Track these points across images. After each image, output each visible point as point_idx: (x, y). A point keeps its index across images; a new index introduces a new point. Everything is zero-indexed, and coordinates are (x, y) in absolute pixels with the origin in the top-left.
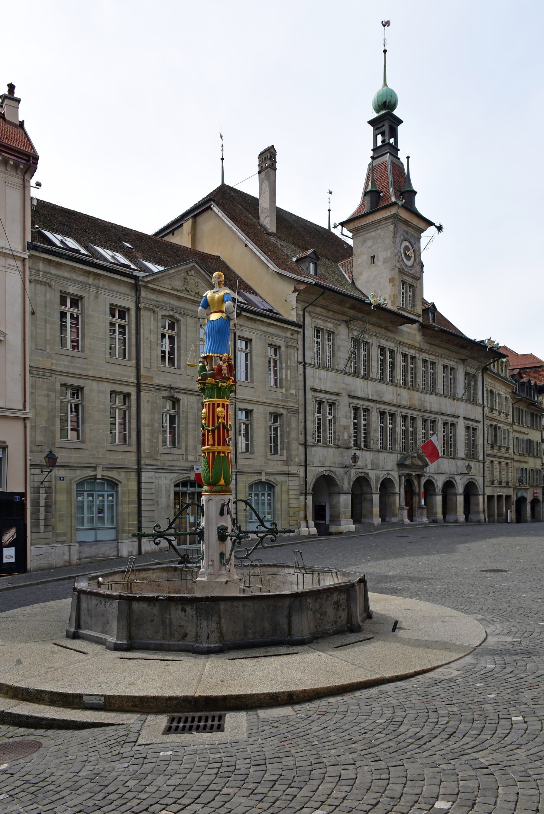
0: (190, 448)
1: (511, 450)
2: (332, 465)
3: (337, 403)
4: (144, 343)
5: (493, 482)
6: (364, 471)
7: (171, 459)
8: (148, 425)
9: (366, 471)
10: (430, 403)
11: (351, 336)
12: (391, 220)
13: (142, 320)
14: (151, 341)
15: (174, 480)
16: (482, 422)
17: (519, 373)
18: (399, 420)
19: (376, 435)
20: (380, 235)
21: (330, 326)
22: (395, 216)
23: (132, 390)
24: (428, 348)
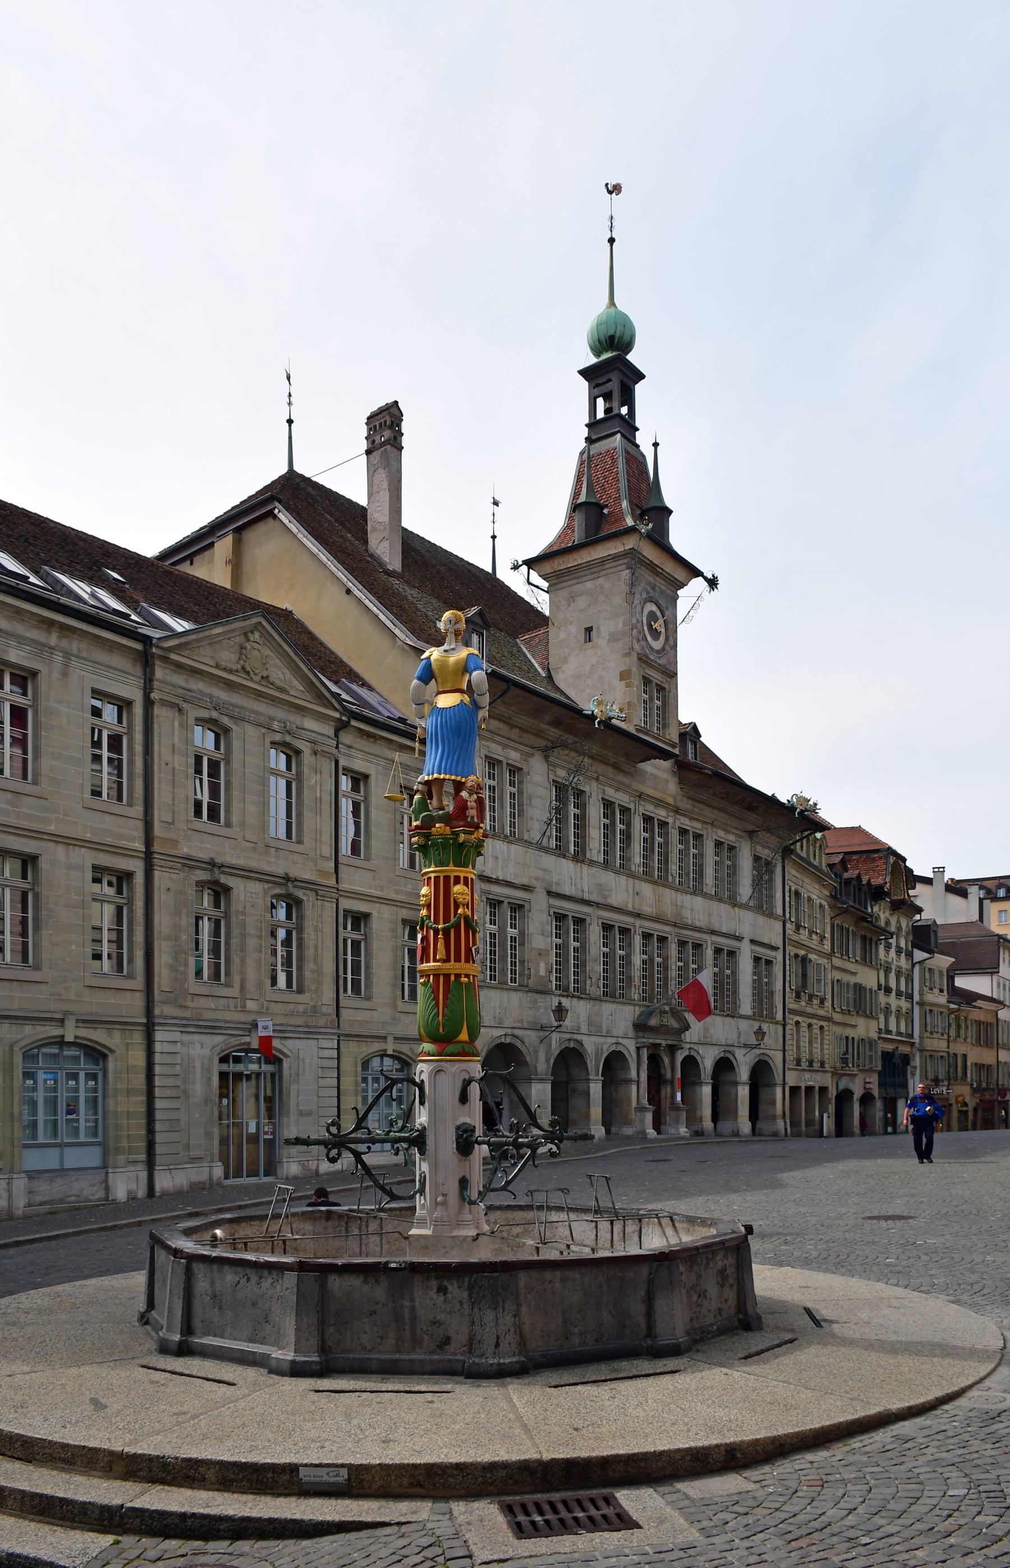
0: (250, 986)
1: (828, 1004)
2: (516, 1025)
3: (527, 906)
4: (160, 772)
5: (798, 1062)
6: (575, 1037)
7: (213, 1007)
8: (168, 938)
9: (579, 1037)
10: (692, 910)
11: (552, 777)
12: (625, 561)
13: (156, 726)
14: (174, 768)
15: (218, 1049)
16: (781, 950)
17: (843, 862)
18: (637, 940)
19: (596, 968)
20: (602, 587)
21: (514, 756)
22: (632, 553)
23: (137, 867)
24: (689, 807)
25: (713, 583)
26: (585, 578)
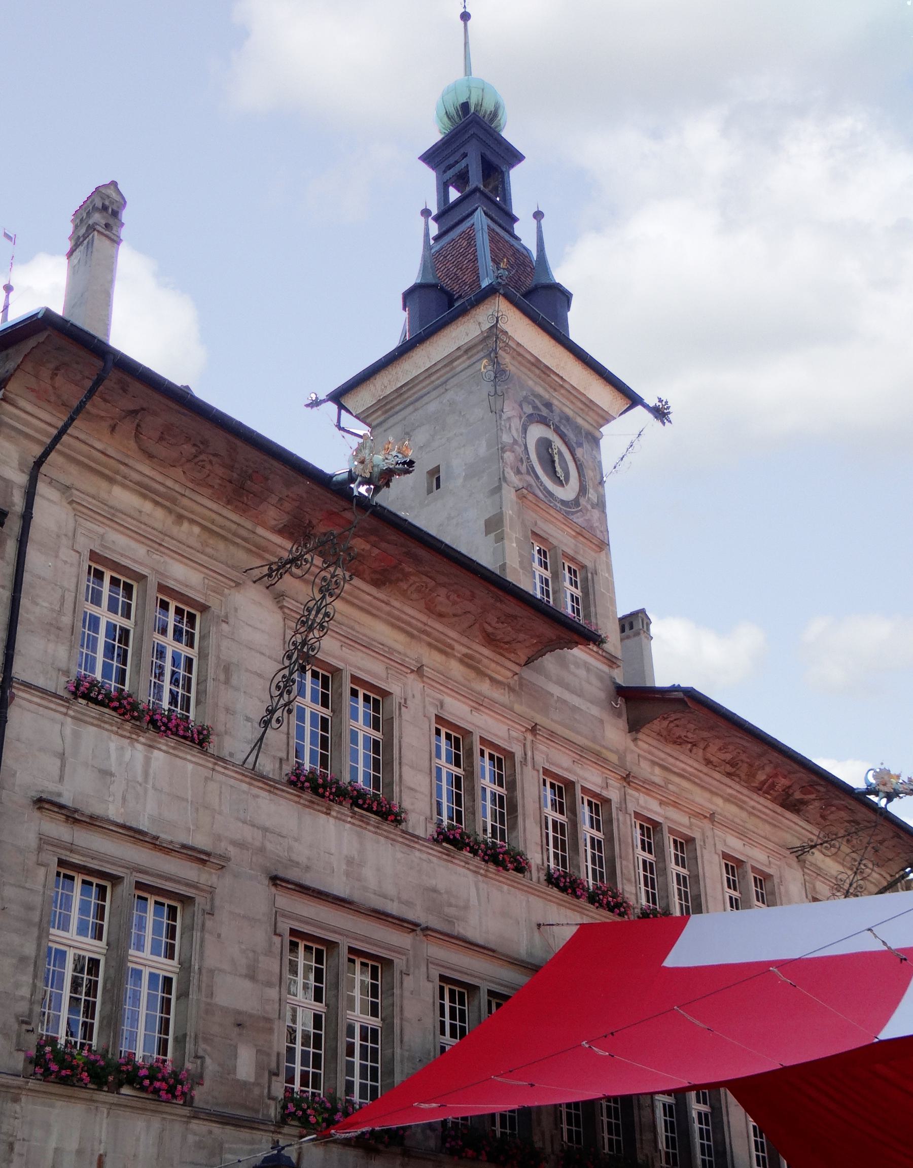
3: (201, 901)
21: (184, 576)
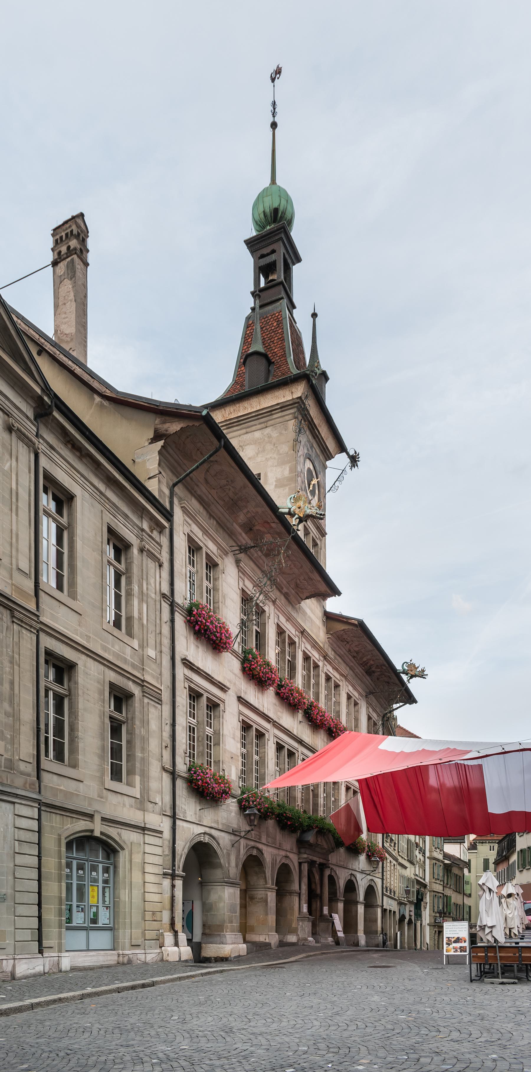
11: (241, 585)
20: (269, 436)
25: (354, 460)
26: (254, 428)
